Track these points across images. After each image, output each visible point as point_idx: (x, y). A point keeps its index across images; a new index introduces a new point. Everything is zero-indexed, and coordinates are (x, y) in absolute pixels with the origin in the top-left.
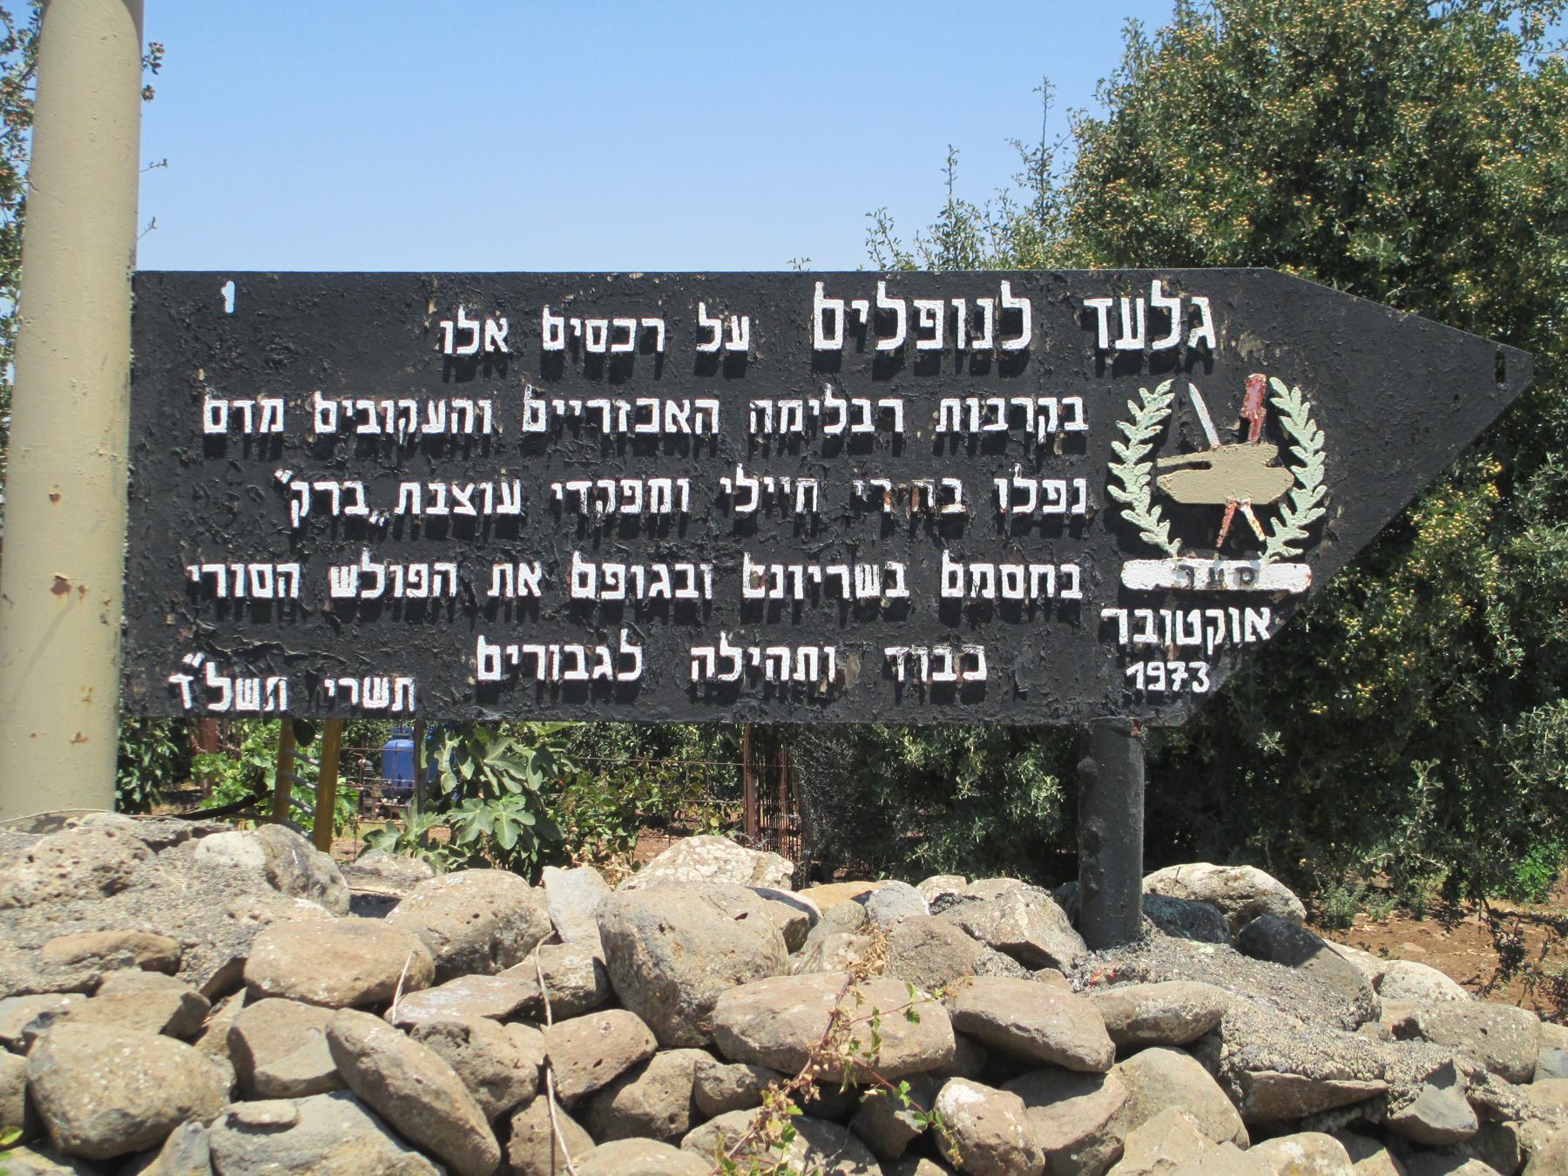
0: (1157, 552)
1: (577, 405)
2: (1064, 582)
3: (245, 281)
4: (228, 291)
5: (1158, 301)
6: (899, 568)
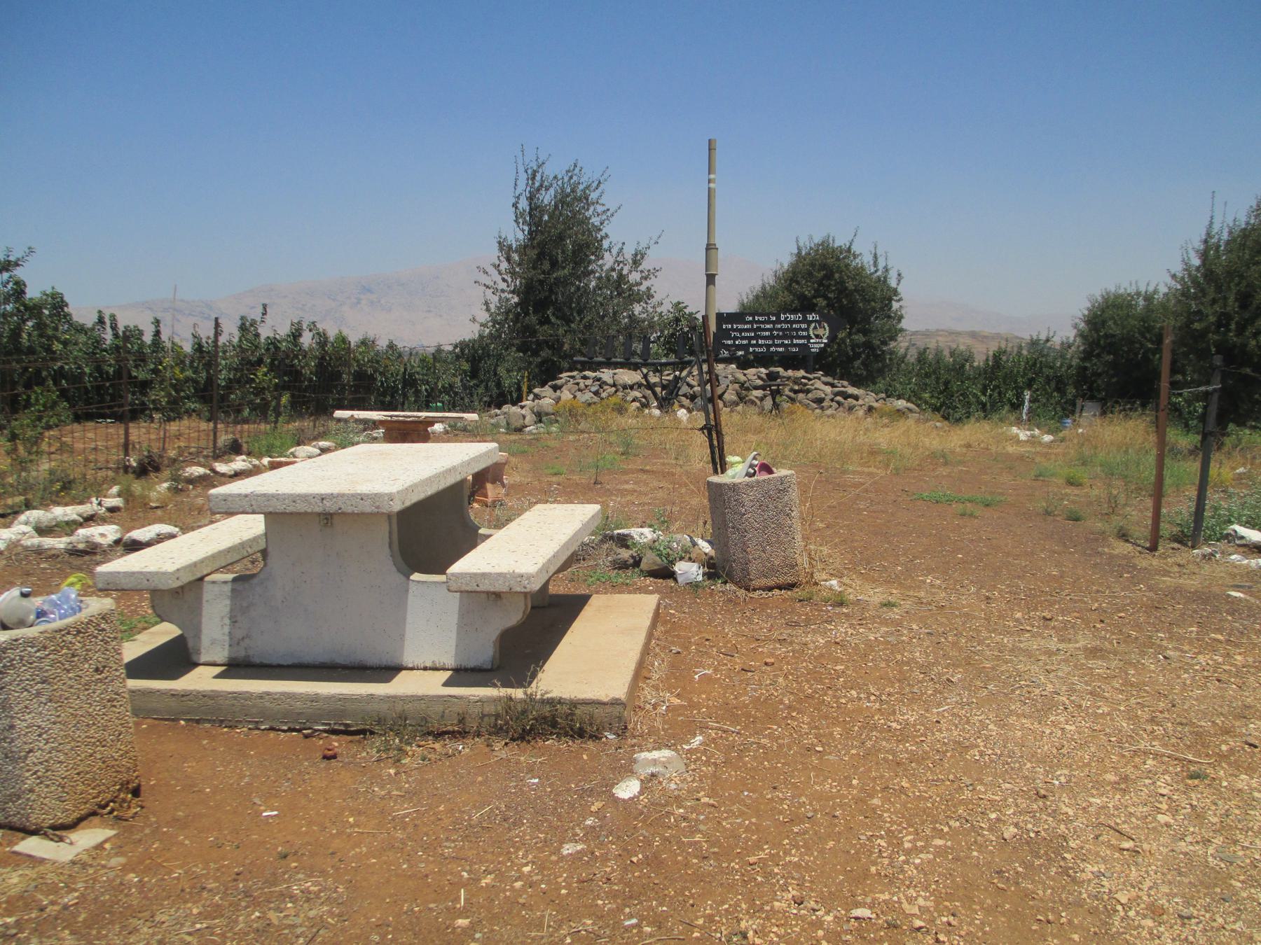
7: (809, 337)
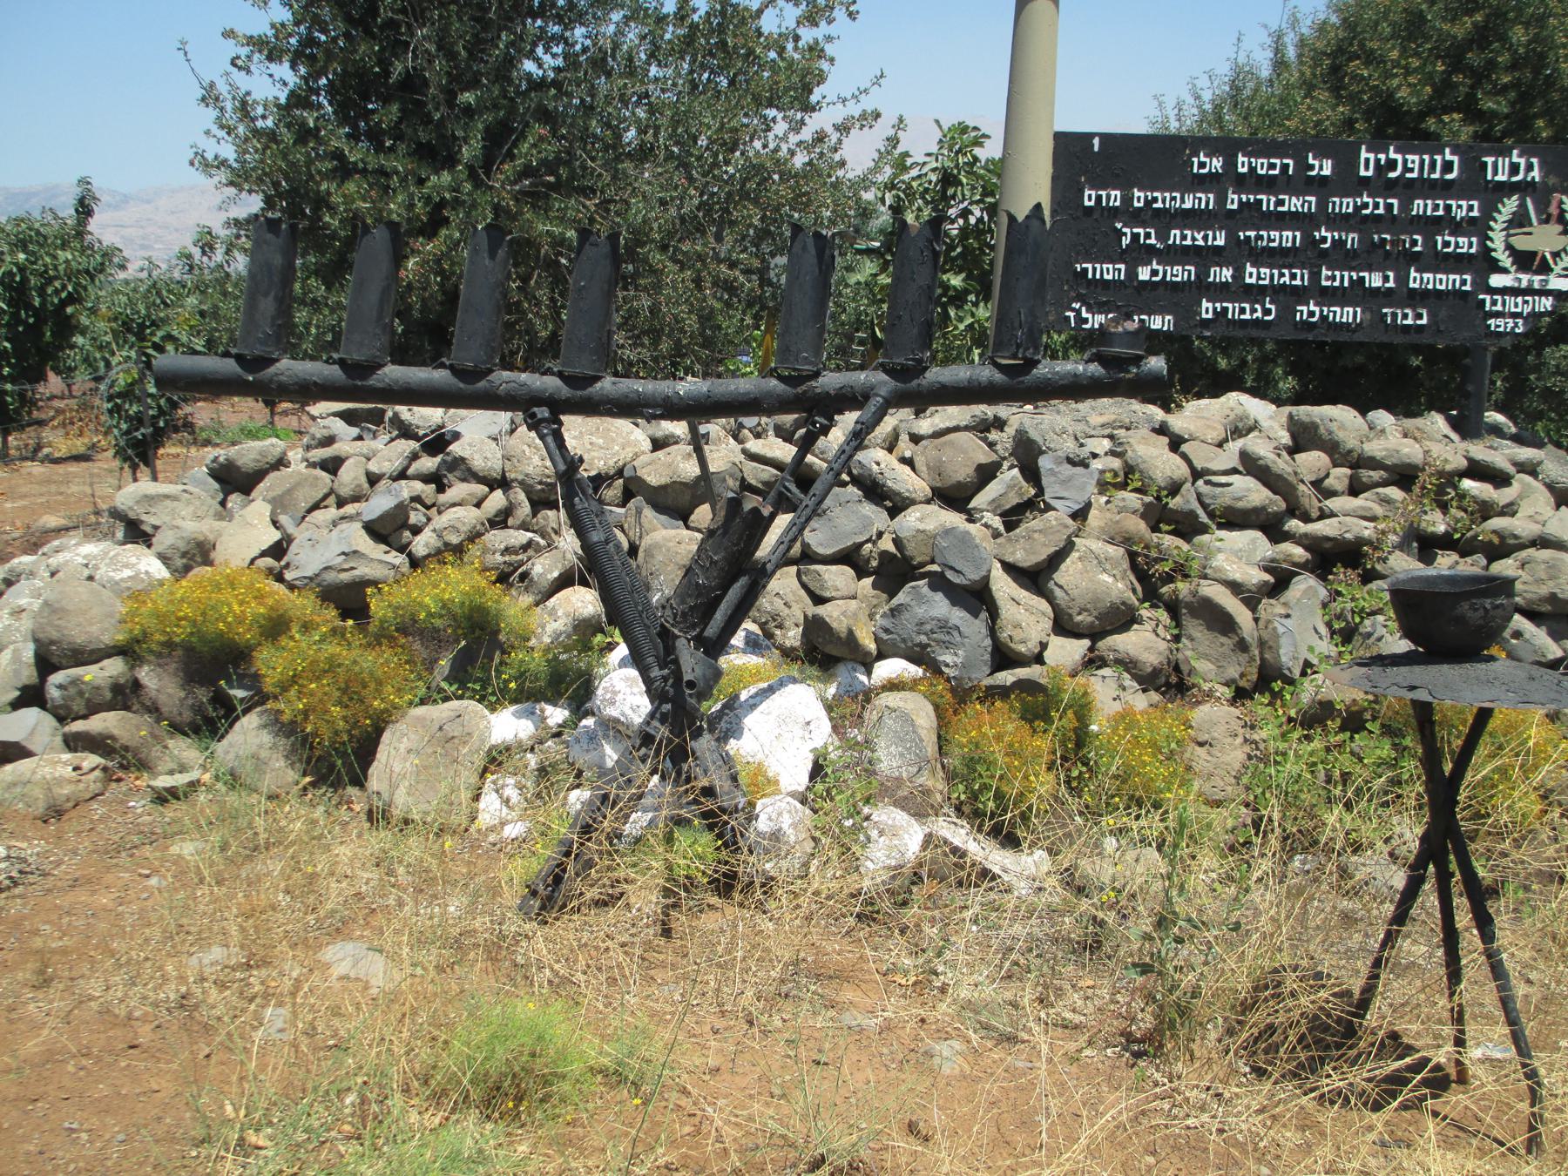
0: (1505, 271)
1: (1252, 198)
2: (1464, 282)
3: (1105, 137)
4: (1096, 141)
5: (1515, 159)
6: (1391, 274)
7: (1485, 263)
